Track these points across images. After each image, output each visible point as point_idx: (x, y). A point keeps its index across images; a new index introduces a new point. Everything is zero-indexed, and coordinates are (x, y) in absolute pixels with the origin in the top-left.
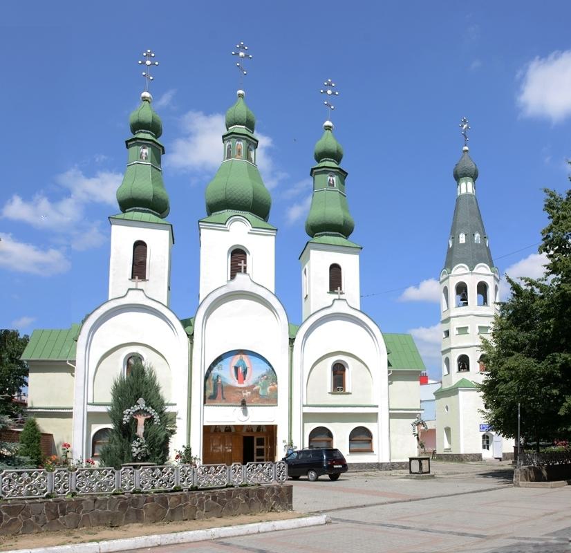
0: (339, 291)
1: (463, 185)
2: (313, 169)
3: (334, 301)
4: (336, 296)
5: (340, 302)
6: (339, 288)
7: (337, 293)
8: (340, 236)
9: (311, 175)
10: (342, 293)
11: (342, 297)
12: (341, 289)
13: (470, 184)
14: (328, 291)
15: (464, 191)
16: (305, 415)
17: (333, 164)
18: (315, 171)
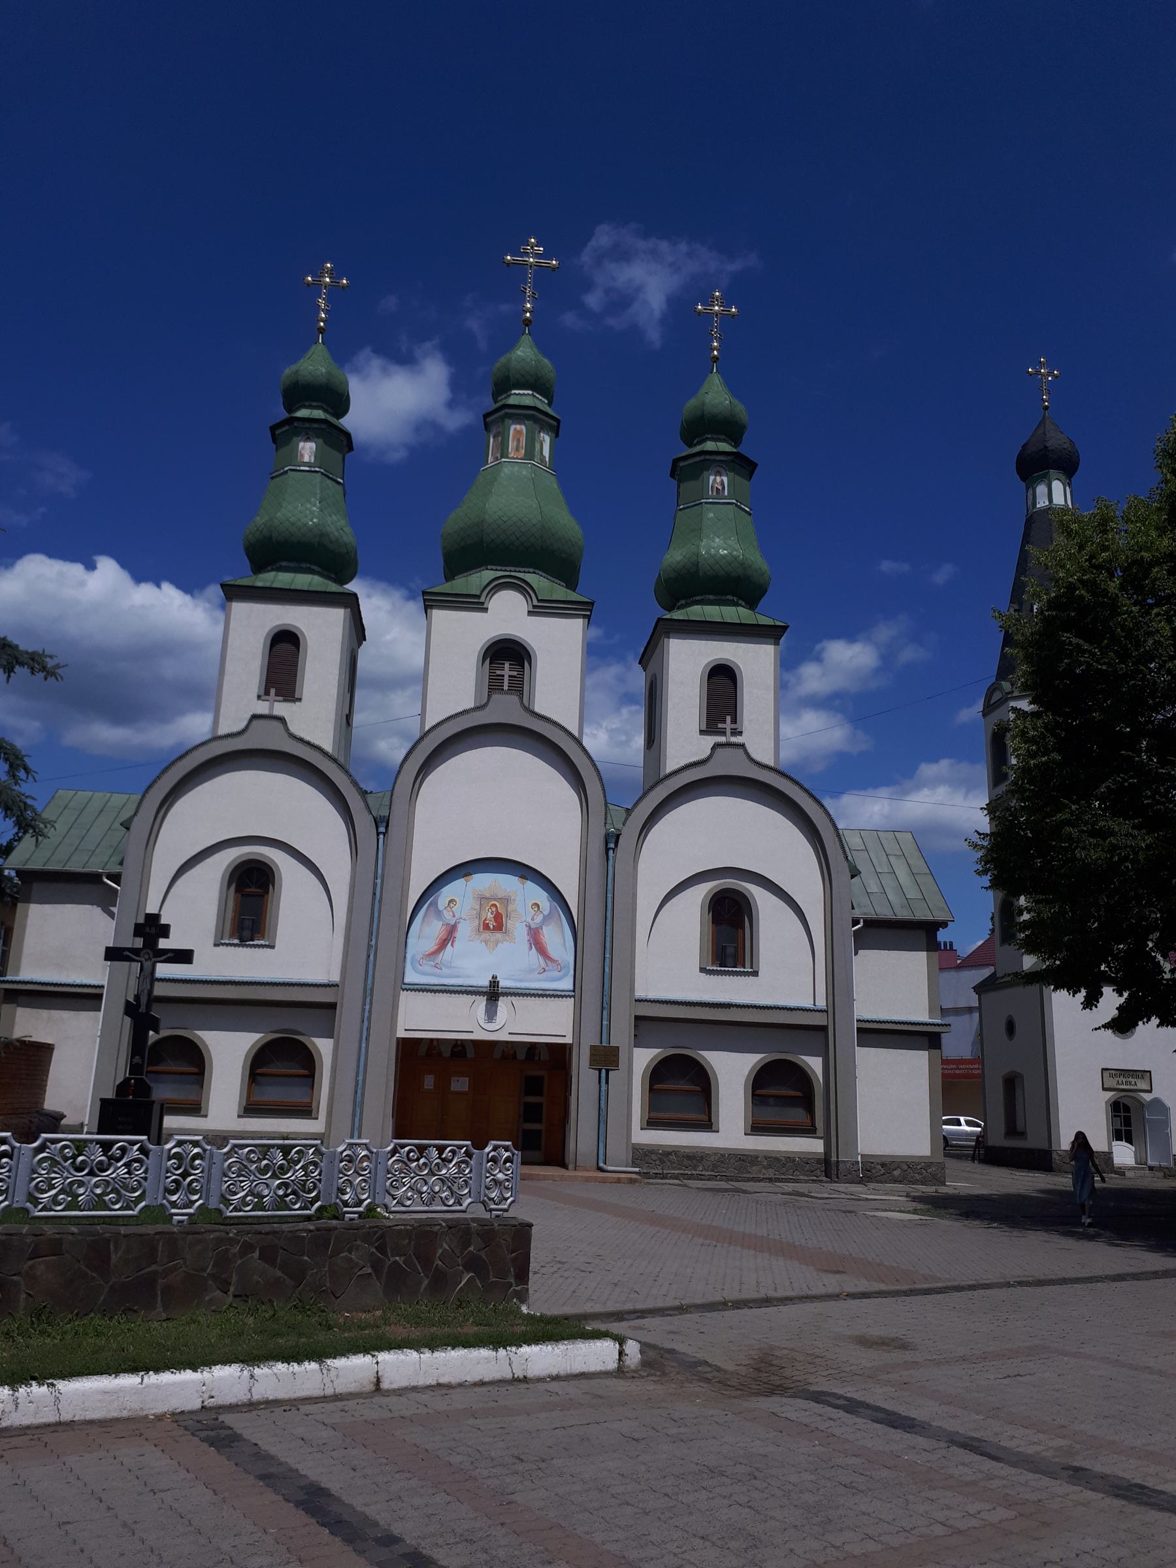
0: (728, 725)
1: (1041, 489)
2: (676, 462)
3: (713, 748)
4: (722, 739)
5: (728, 750)
6: (728, 718)
7: (723, 733)
8: (736, 605)
9: (672, 475)
10: (737, 732)
11: (734, 739)
12: (734, 721)
13: (1057, 486)
14: (704, 728)
15: (1042, 503)
16: (638, 1018)
17: (724, 447)
18: (682, 464)
